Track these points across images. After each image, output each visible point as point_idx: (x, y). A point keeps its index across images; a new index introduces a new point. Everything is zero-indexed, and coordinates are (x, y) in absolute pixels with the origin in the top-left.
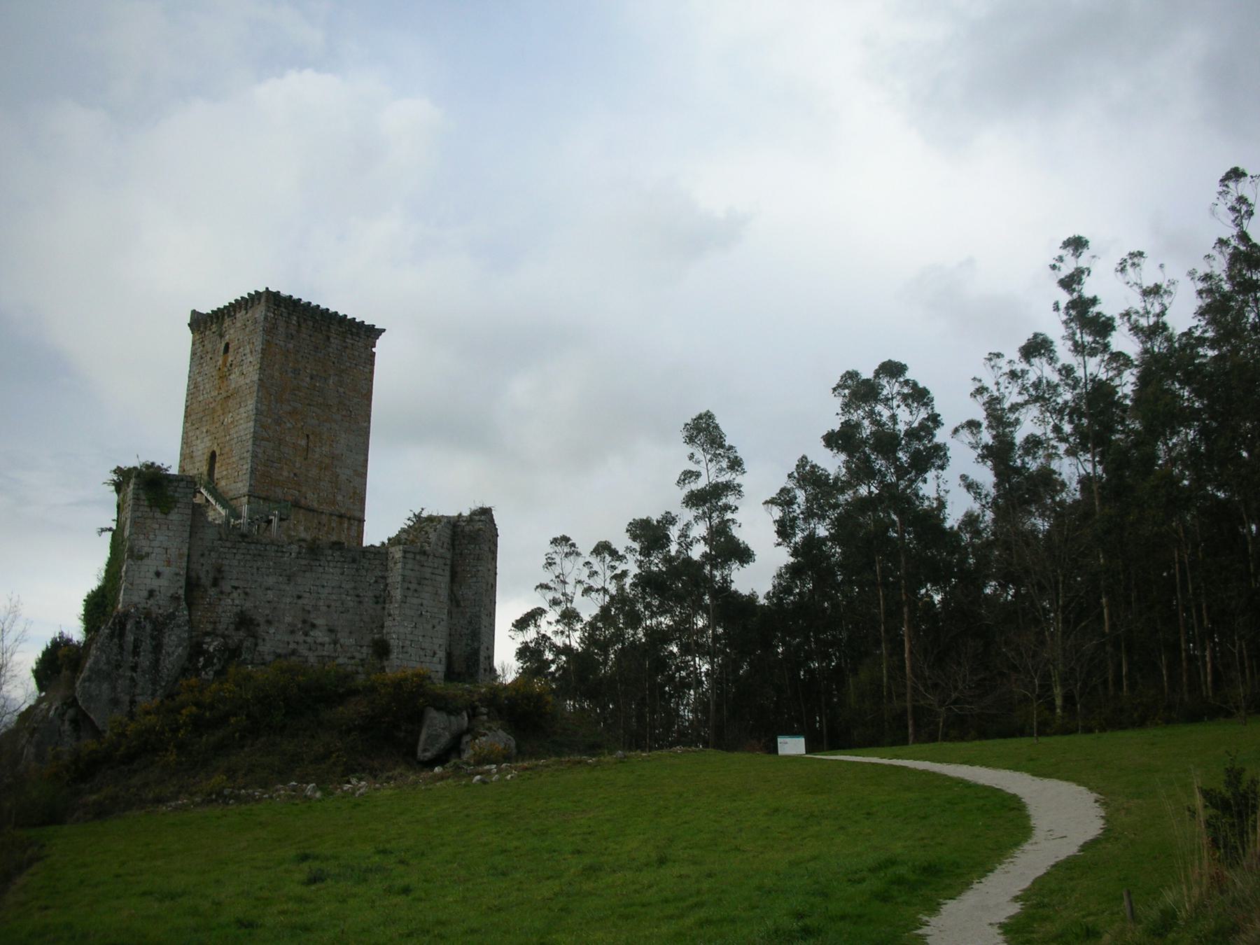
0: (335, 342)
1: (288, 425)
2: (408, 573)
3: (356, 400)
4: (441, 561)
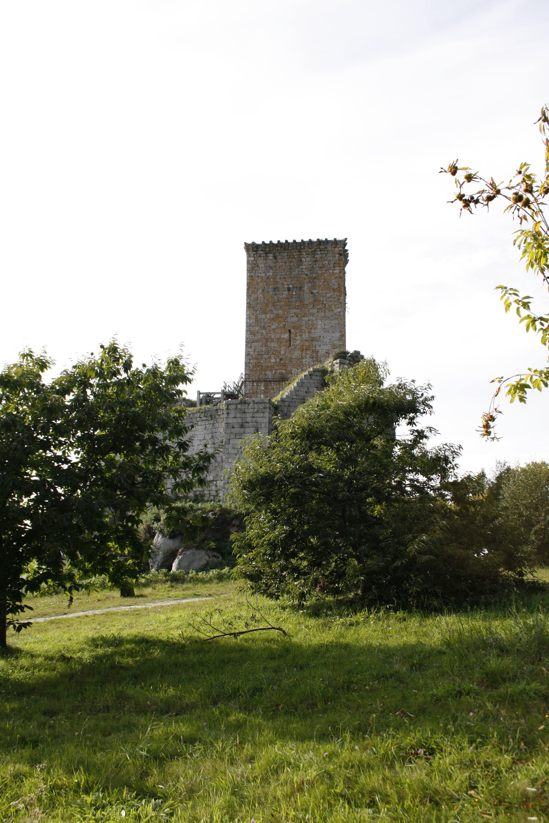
0: (307, 260)
1: (273, 327)
2: (230, 421)
3: (329, 295)
4: (261, 406)
